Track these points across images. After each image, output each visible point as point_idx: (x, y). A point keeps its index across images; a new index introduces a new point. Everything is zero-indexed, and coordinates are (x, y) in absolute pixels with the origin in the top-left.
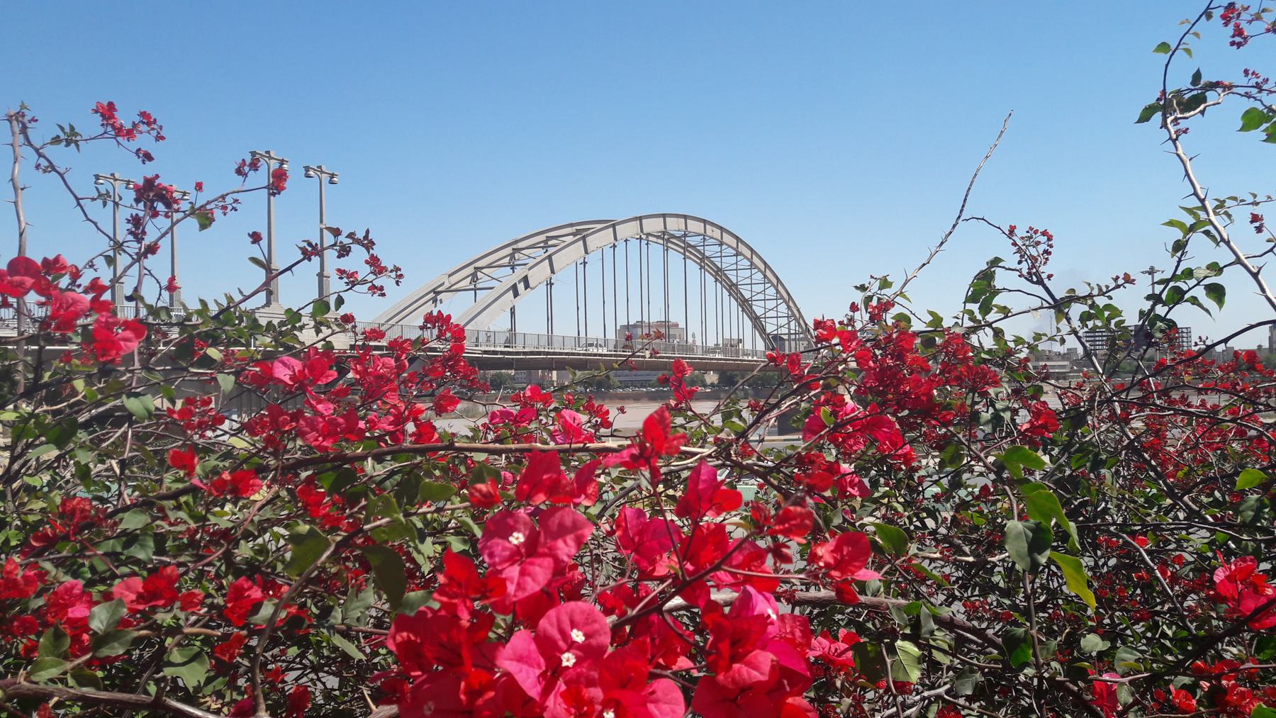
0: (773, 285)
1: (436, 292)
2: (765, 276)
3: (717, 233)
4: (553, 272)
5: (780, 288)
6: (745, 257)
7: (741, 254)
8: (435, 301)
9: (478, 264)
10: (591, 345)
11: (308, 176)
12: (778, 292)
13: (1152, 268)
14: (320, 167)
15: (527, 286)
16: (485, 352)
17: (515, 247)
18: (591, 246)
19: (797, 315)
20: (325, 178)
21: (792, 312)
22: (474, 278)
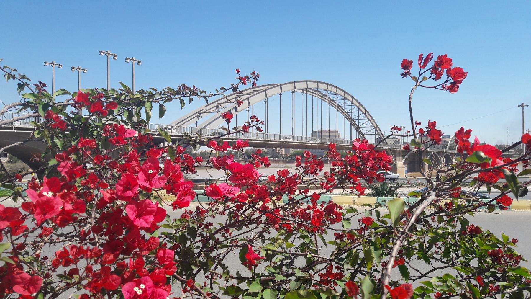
0: (363, 113)
1: (199, 113)
2: (359, 109)
3: (334, 89)
5: (367, 114)
6: (349, 100)
7: (347, 99)
8: (198, 117)
9: (219, 102)
10: (286, 138)
12: (365, 115)
13: (523, 104)
14: (132, 58)
15: (236, 111)
19: (376, 126)
21: (373, 124)
22: (217, 107)
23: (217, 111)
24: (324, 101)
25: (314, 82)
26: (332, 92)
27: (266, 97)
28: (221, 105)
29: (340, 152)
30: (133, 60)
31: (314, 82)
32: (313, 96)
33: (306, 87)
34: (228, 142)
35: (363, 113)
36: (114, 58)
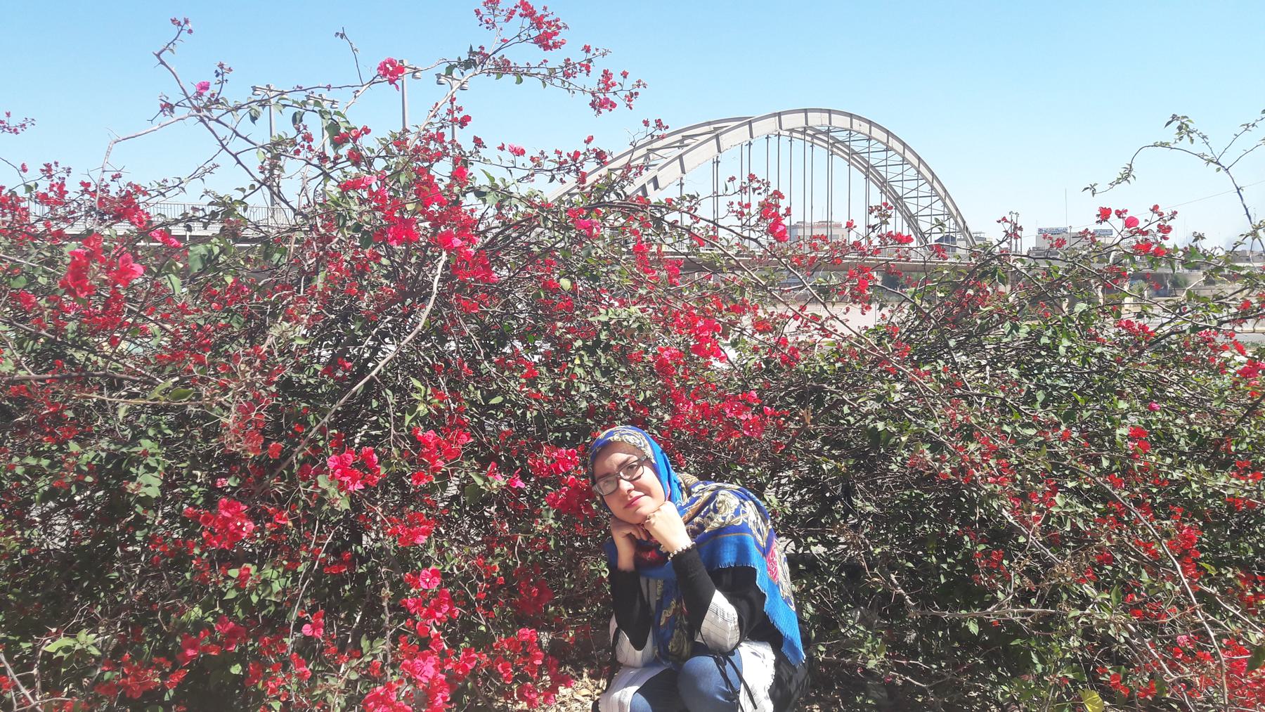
0: (927, 181)
2: (919, 172)
3: (865, 128)
4: (683, 172)
6: (897, 153)
7: (892, 149)
12: (933, 188)
15: (656, 187)
24: (838, 154)
25: (821, 111)
31: (821, 111)
33: (804, 125)
35: (927, 181)
36: (414, 76)
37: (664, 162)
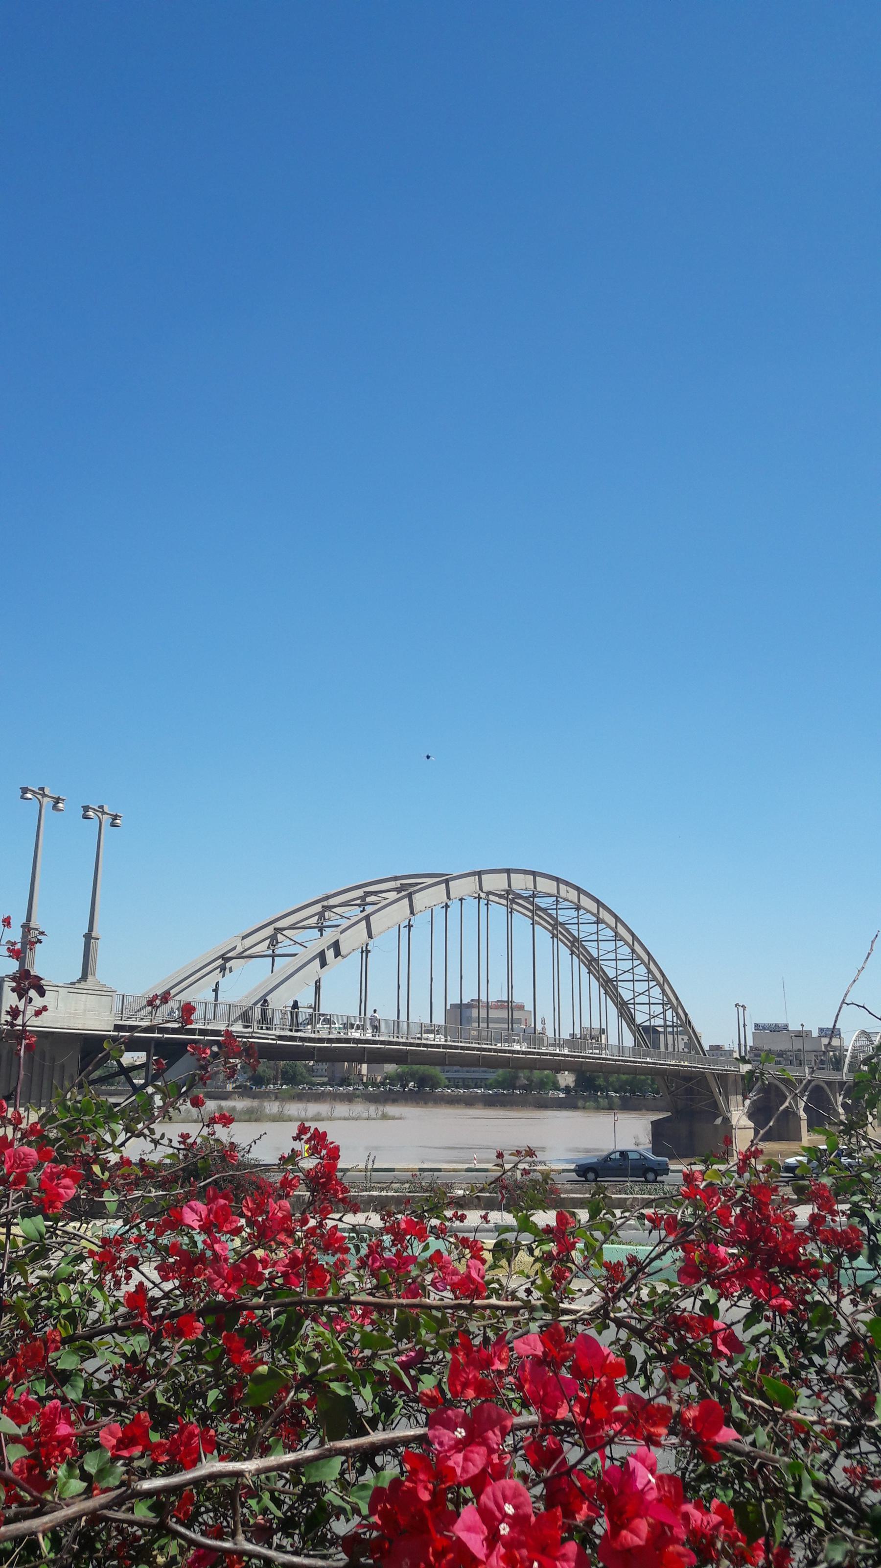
0: (643, 962)
1: (225, 958)
2: (633, 951)
3: (573, 895)
4: (370, 936)
5: (652, 966)
6: (608, 926)
7: (603, 922)
8: (223, 969)
9: (279, 925)
11: (86, 817)
12: (649, 971)
14: (101, 807)
15: (337, 954)
16: (281, 1038)
17: (325, 903)
18: (417, 906)
20: (107, 819)
22: (273, 940)
23: (270, 952)
24: (539, 924)
25: (525, 872)
26: (568, 900)
27: (412, 913)
28: (284, 933)
29: (613, 1078)
30: (104, 813)
31: (525, 872)
32: (512, 909)
34: (314, 1047)
35: (643, 962)
36: (55, 807)
37: (351, 922)
